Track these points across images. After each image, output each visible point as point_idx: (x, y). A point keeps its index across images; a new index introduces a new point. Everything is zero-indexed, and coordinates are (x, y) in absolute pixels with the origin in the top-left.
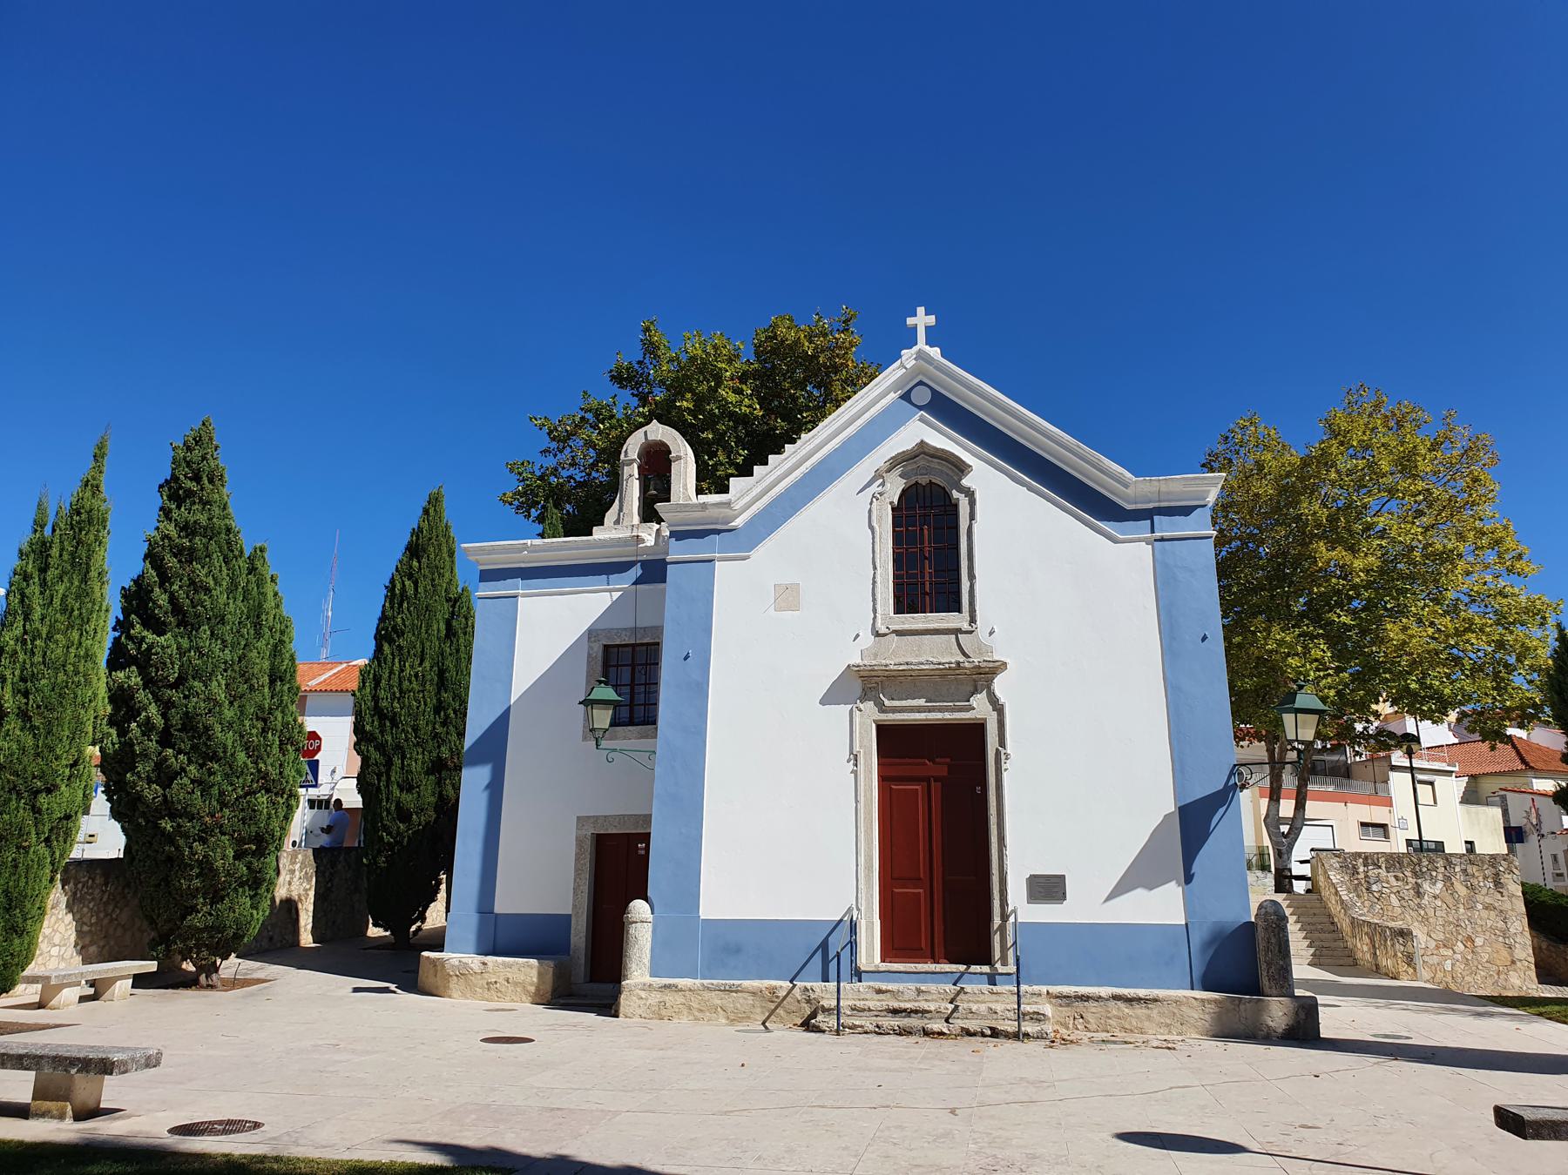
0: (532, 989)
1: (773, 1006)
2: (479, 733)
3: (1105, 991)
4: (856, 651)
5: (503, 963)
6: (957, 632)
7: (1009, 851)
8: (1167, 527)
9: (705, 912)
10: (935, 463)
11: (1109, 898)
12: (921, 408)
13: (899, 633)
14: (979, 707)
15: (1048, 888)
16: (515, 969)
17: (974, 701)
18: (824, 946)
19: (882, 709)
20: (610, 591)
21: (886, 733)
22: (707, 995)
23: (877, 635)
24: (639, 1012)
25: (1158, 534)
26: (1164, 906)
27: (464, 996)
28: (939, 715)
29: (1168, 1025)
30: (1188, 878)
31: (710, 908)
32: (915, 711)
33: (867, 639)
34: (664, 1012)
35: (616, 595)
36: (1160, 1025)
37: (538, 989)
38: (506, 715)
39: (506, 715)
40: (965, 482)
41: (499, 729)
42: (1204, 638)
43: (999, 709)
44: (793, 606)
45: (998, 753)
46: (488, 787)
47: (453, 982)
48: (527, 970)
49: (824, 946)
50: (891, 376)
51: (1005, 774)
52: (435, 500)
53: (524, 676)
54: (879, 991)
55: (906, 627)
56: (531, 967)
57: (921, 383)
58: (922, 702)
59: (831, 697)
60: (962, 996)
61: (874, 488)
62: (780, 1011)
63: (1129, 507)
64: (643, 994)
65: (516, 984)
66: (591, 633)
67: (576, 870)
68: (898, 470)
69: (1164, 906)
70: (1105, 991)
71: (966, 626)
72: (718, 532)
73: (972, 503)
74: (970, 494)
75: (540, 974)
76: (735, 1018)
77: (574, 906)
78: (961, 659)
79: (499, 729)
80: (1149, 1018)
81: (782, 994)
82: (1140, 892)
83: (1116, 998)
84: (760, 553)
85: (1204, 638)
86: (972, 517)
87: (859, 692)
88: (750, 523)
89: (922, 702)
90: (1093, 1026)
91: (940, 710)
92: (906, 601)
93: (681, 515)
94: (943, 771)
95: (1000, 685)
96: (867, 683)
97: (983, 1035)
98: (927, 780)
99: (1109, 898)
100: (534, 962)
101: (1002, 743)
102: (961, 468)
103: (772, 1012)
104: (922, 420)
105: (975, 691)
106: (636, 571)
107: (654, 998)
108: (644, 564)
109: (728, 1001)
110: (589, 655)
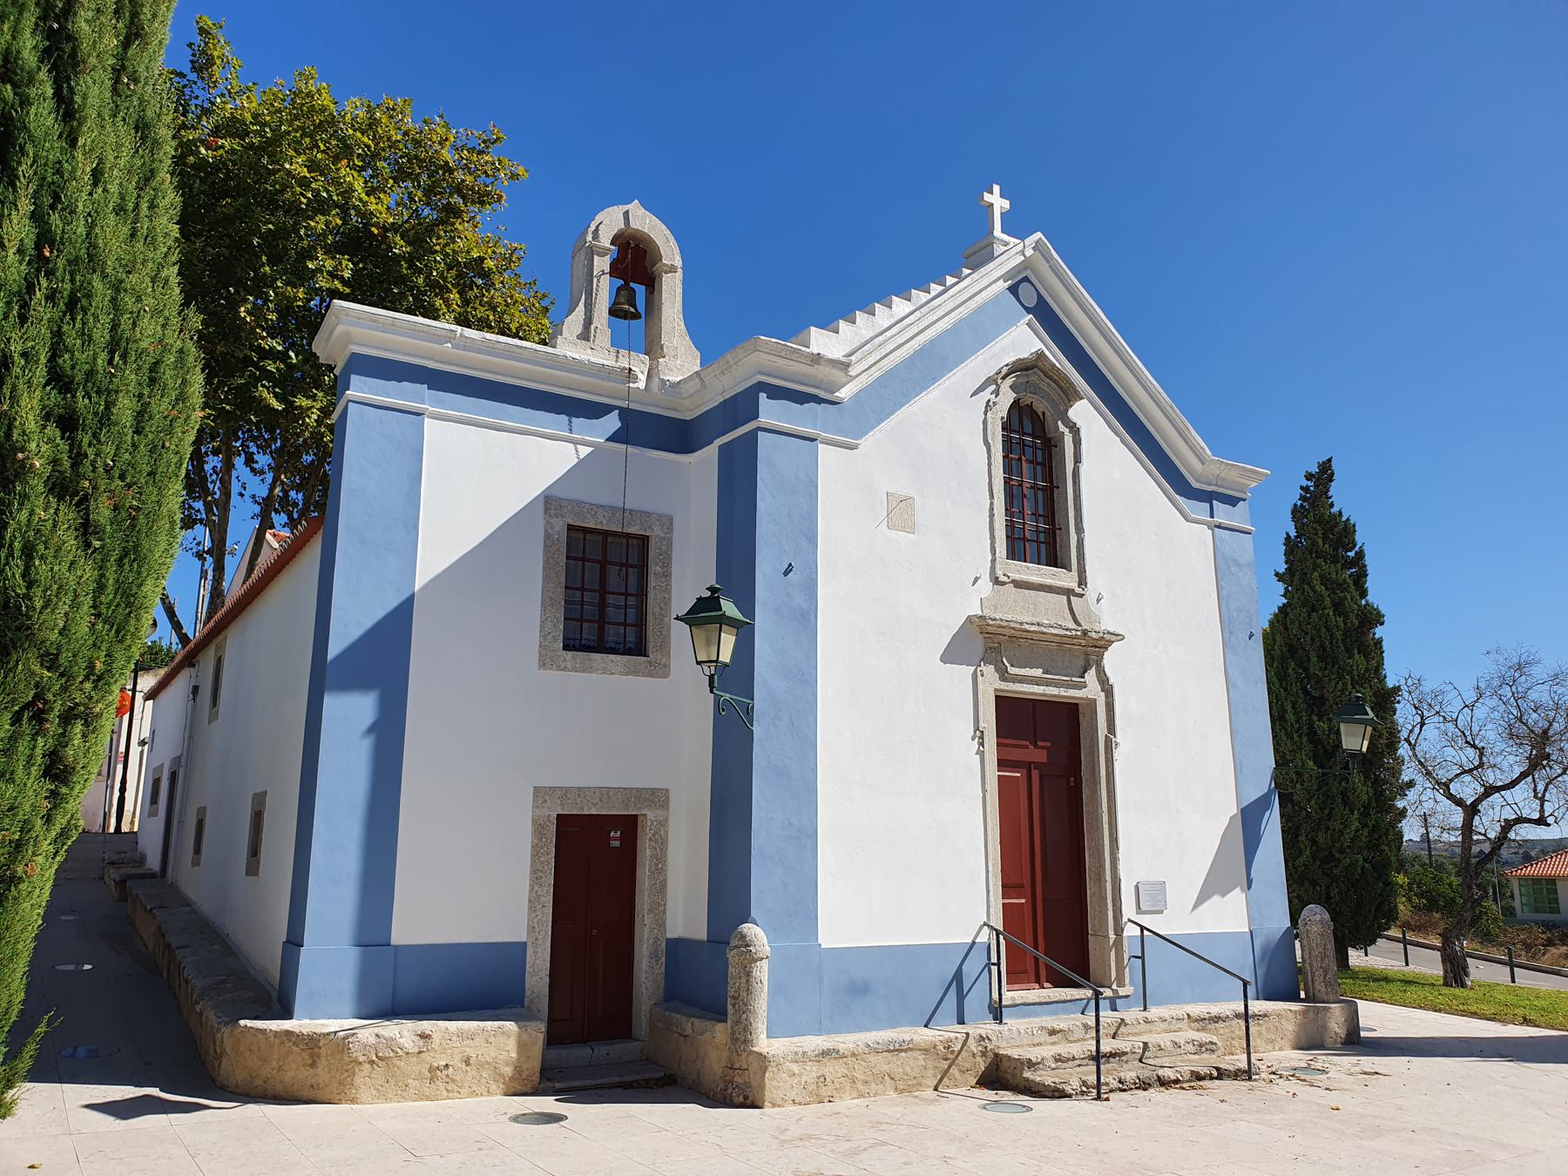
0: (508, 1071)
1: (945, 1064)
2: (356, 633)
4: (974, 600)
5: (460, 1034)
6: (1069, 593)
7: (1122, 855)
8: (1223, 513)
9: (830, 936)
10: (1045, 385)
11: (1195, 907)
13: (1018, 584)
14: (1091, 689)
16: (479, 1040)
18: (958, 976)
19: (1004, 675)
20: (575, 442)
21: (1005, 705)
22: (873, 1058)
23: (996, 581)
24: (792, 1095)
25: (1217, 520)
27: (383, 1096)
28: (1063, 692)
29: (1273, 1041)
31: (830, 936)
32: (1034, 684)
33: (986, 586)
34: (824, 1092)
35: (585, 451)
37: (518, 1070)
38: (404, 612)
39: (404, 612)
41: (395, 631)
43: (1108, 691)
44: (909, 527)
45: (1108, 742)
46: (371, 730)
47: (362, 1077)
48: (499, 1041)
49: (958, 976)
53: (435, 554)
54: (1053, 1032)
55: (1049, 581)
56: (506, 1034)
57: (1026, 279)
58: (1038, 672)
59: (949, 657)
60: (1123, 1029)
61: (987, 394)
62: (954, 1071)
63: (1195, 485)
64: (795, 1068)
65: (481, 1066)
66: (549, 502)
67: (534, 871)
68: (1010, 381)
71: (1074, 585)
73: (1077, 443)
74: (1075, 430)
75: (522, 1046)
76: (907, 1087)
77: (531, 929)
78: (1072, 625)
79: (395, 631)
81: (957, 1048)
82: (1216, 898)
84: (868, 442)
86: (1077, 459)
87: (980, 652)
88: (856, 397)
89: (1038, 672)
91: (1048, 683)
92: (1018, 547)
93: (781, 362)
94: (1040, 756)
96: (987, 642)
97: (1212, 1078)
99: (1195, 907)
100: (510, 1026)
101: (1111, 728)
103: (945, 1073)
106: (612, 422)
107: (811, 1071)
108: (625, 414)
109: (896, 1065)
110: (547, 536)
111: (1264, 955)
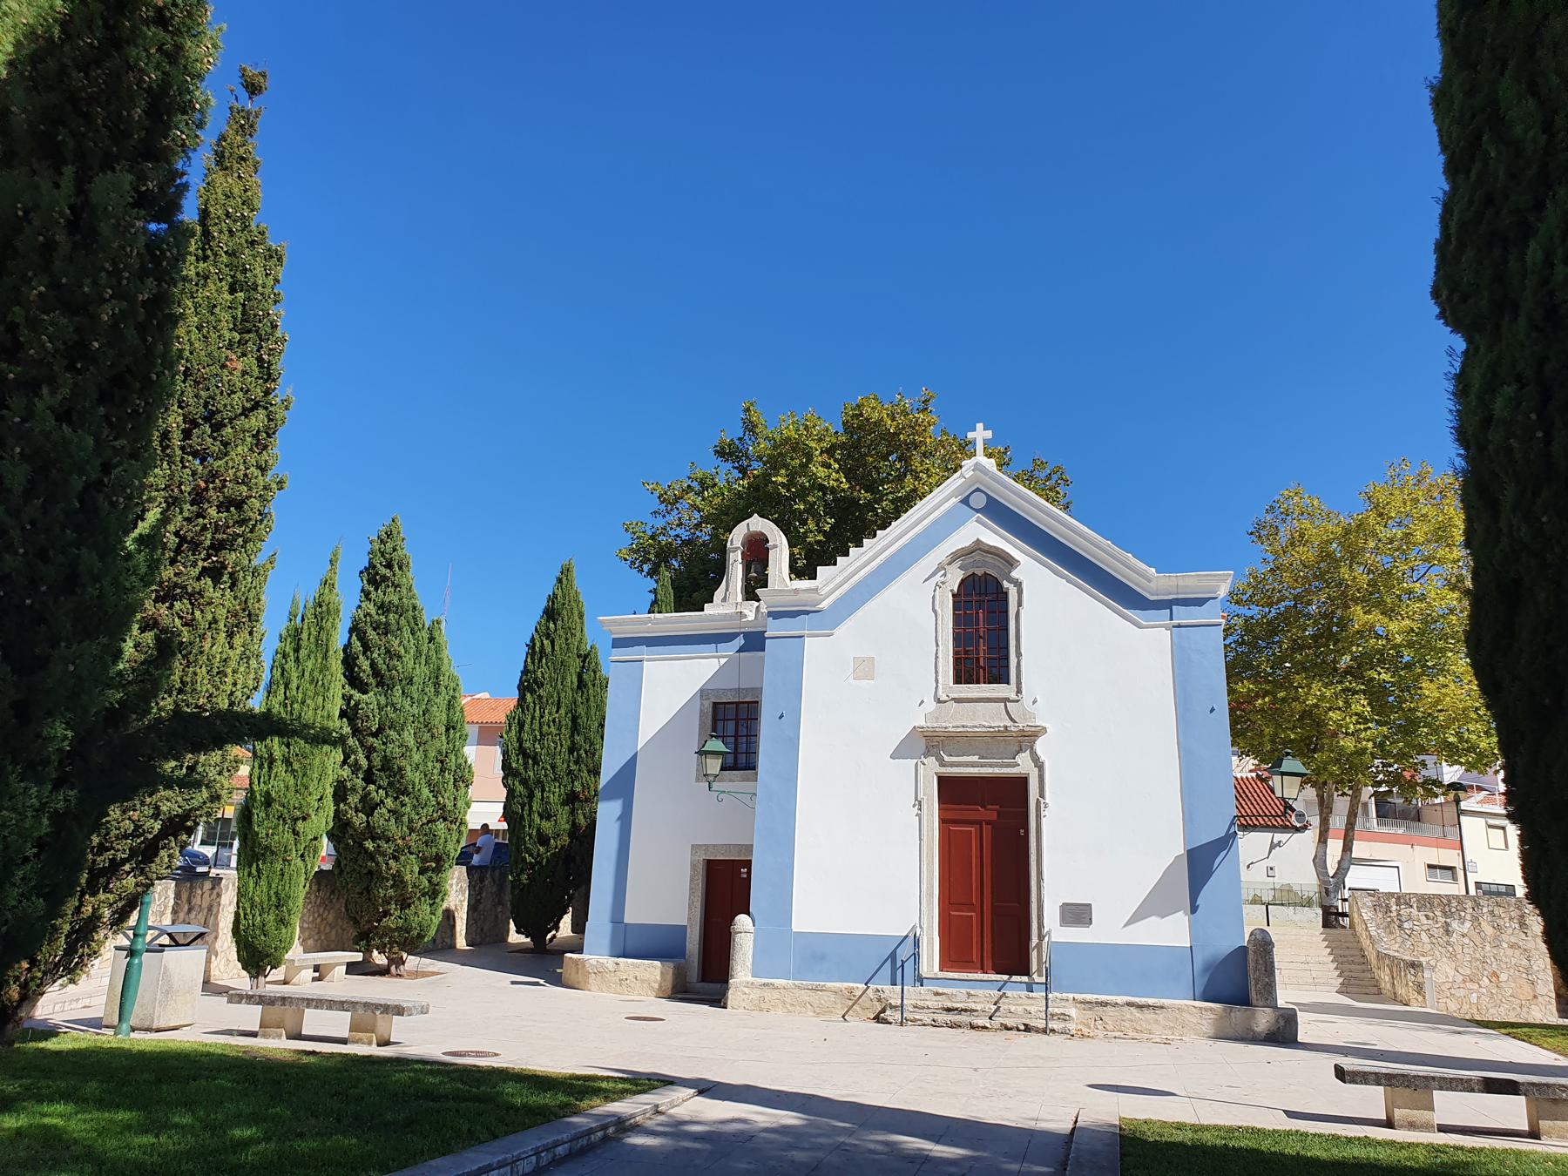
3: (1121, 999)
6: (1006, 700)
7: (1046, 884)
8: (1183, 615)
10: (989, 558)
12: (977, 511)
15: (1077, 914)
17: (1019, 759)
18: (893, 956)
19: (943, 764)
21: (943, 782)
22: (798, 992)
23: (939, 701)
25: (1175, 622)
26: (1173, 931)
28: (990, 770)
30: (1194, 909)
32: (970, 766)
33: (931, 705)
35: (723, 661)
36: (1165, 1027)
38: (633, 761)
39: (633, 761)
40: (1014, 574)
41: (628, 771)
42: (1212, 710)
43: (1040, 766)
44: (869, 676)
48: (653, 971)
49: (893, 956)
50: (954, 482)
51: (1044, 820)
52: (566, 571)
54: (937, 994)
55: (963, 695)
57: (978, 490)
58: (975, 758)
61: (938, 578)
63: (1152, 598)
65: (643, 981)
66: (703, 692)
69: (1173, 931)
70: (1121, 999)
71: (1013, 696)
72: (808, 613)
73: (1020, 592)
74: (1018, 584)
78: (1009, 723)
79: (628, 771)
80: (1156, 1022)
82: (1153, 920)
83: (1129, 1004)
84: (841, 631)
85: (1212, 710)
86: (1020, 604)
89: (975, 758)
90: (1110, 1027)
92: (965, 672)
94: (994, 816)
95: (1040, 746)
96: (931, 742)
98: (979, 823)
101: (1042, 794)
102: (1011, 563)
104: (978, 521)
105: (1020, 751)
106: (740, 641)
108: (746, 635)
109: (814, 997)
111: (1205, 970)
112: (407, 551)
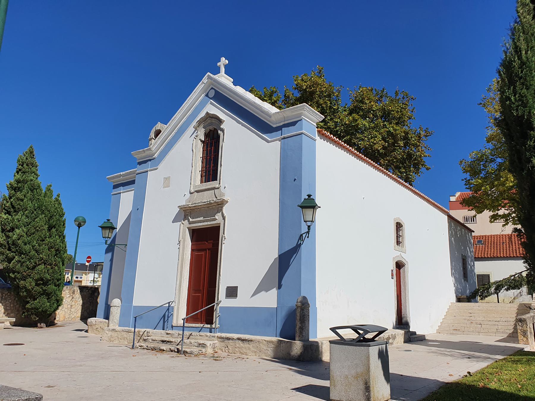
3: (236, 336)
6: (214, 189)
7: (221, 278)
9: (135, 303)
12: (211, 99)
15: (232, 292)
17: (217, 217)
22: (123, 333)
26: (269, 299)
30: (280, 287)
34: (112, 339)
36: (252, 351)
40: (222, 127)
42: (295, 180)
50: (200, 87)
51: (223, 245)
58: (202, 218)
60: (191, 336)
61: (195, 134)
63: (274, 126)
68: (202, 126)
69: (269, 299)
70: (236, 336)
71: (217, 186)
72: (150, 160)
74: (223, 130)
80: (249, 349)
82: (263, 293)
83: (239, 339)
85: (295, 180)
88: (159, 155)
89: (202, 218)
90: (230, 351)
91: (207, 221)
95: (225, 209)
96: (186, 213)
98: (205, 250)
102: (220, 121)
104: (211, 103)
105: (218, 212)
112: (37, 160)
